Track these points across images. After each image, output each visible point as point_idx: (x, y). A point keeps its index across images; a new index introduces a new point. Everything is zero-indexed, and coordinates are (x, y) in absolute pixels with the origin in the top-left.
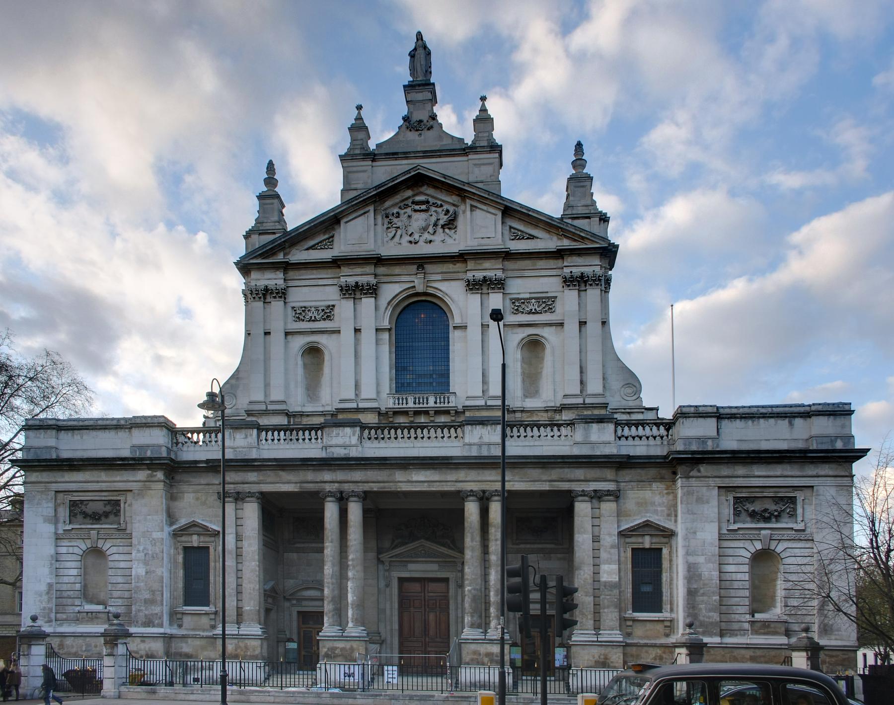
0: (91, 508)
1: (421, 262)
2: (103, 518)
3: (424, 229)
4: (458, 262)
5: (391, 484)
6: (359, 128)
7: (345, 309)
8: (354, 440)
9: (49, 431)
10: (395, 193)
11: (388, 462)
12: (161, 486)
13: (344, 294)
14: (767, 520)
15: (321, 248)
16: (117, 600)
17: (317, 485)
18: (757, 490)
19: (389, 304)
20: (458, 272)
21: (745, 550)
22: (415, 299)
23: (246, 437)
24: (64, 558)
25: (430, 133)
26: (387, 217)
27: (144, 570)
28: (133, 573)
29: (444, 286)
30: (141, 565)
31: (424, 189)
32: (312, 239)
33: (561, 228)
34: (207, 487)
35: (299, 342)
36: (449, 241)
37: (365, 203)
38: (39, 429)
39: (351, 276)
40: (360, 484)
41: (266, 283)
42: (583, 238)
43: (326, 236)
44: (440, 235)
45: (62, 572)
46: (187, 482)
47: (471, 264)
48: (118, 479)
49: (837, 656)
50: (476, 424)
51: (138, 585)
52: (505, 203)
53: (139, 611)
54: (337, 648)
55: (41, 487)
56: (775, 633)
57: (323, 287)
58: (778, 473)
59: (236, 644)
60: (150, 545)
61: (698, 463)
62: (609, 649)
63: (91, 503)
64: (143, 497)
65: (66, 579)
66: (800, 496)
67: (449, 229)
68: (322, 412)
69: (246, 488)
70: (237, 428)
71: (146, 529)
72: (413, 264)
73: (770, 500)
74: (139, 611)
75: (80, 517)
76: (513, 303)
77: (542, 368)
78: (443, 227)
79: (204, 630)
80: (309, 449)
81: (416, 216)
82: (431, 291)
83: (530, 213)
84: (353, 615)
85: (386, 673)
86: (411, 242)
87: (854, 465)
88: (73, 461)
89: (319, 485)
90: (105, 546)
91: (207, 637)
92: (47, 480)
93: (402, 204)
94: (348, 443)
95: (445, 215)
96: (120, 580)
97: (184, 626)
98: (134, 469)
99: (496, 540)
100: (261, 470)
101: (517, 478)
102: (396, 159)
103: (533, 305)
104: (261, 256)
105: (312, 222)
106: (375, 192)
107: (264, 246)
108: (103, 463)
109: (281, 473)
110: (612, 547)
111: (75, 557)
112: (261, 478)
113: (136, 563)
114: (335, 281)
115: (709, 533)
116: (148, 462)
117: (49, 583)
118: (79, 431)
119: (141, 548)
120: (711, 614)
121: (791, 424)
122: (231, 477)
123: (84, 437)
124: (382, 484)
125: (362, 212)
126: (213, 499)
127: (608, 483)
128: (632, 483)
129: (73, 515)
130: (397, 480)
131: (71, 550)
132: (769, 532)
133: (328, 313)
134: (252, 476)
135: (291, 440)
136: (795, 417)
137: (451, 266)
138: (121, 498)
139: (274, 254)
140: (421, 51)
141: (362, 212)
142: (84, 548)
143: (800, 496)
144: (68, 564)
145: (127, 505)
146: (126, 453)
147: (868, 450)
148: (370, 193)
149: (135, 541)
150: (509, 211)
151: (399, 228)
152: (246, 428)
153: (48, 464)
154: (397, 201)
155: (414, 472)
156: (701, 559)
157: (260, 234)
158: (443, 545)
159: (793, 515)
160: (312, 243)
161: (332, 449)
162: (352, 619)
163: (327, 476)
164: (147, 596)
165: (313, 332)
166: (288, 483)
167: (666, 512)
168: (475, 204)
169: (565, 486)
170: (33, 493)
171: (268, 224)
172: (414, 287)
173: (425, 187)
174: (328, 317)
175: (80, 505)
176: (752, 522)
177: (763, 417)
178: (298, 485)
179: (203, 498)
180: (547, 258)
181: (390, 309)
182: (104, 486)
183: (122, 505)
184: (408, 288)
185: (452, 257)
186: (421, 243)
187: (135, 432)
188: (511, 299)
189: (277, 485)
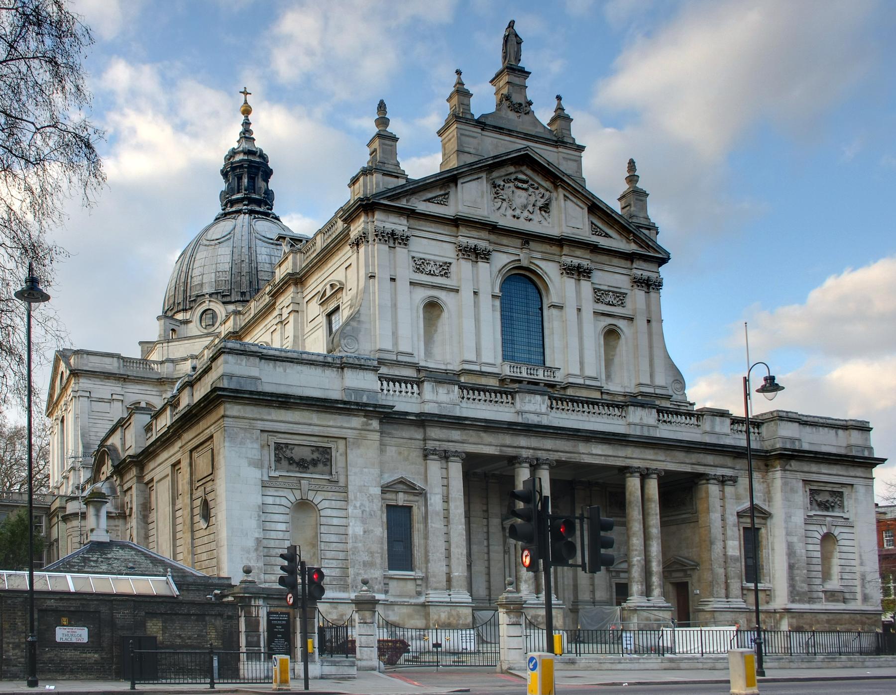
0: (298, 453)
1: (527, 238)
2: (310, 466)
3: (525, 207)
4: (554, 244)
5: (576, 455)
6: (461, 93)
7: (463, 269)
8: (544, 408)
9: (252, 358)
11: (579, 434)
12: (376, 436)
14: (827, 509)
15: (438, 203)
16: (331, 561)
17: (514, 449)
18: (822, 484)
19: (500, 271)
20: (555, 255)
21: (818, 532)
22: (516, 272)
23: (448, 393)
24: (270, 509)
25: (526, 117)
26: (495, 187)
27: (362, 528)
28: (350, 531)
29: (542, 264)
30: (359, 523)
31: (524, 168)
33: (634, 234)
34: (410, 441)
35: (422, 294)
36: (544, 223)
37: (481, 169)
38: (241, 354)
40: (551, 453)
41: (394, 227)
42: (649, 246)
43: (442, 192)
44: (537, 216)
45: (269, 526)
46: (389, 434)
47: (566, 250)
48: (331, 423)
49: (871, 618)
50: (637, 406)
51: (356, 545)
52: (594, 201)
53: (358, 574)
54: (539, 616)
55: (243, 424)
56: (837, 601)
57: (440, 243)
58: (834, 472)
59: (448, 612)
60: (367, 502)
61: (791, 459)
62: (738, 614)
63: (296, 447)
64: (359, 447)
65: (273, 535)
66: (846, 491)
68: (446, 370)
69: (451, 447)
70: (440, 382)
71: (362, 483)
72: (519, 238)
73: (827, 493)
74: (358, 574)
75: (284, 463)
76: (595, 292)
77: (613, 355)
78: (540, 209)
79: (411, 597)
80: (502, 412)
81: (519, 192)
82: (533, 267)
83: (613, 215)
85: (624, 639)
86: (514, 216)
87: (874, 470)
88: (290, 398)
89: (517, 450)
90: (317, 498)
91: (415, 605)
92: (250, 416)
93: (506, 178)
94: (538, 411)
96: (333, 538)
97: (390, 591)
98: (349, 415)
99: (656, 514)
100: (465, 429)
101: (668, 459)
102: (501, 134)
104: (388, 198)
106: (492, 162)
107: (395, 189)
108: (323, 404)
109: (483, 434)
110: (734, 525)
111: (282, 510)
112: (465, 438)
113: (353, 521)
114: (453, 240)
115: (799, 517)
116: (371, 409)
117: (257, 538)
118: (281, 363)
119: (358, 505)
120: (803, 585)
121: (837, 434)
122: (435, 432)
123: (288, 371)
124: (569, 455)
125: (476, 176)
126: (416, 455)
127: (728, 469)
128: (741, 471)
129: (278, 460)
130: (581, 451)
131: (278, 500)
132: (831, 519)
133: (445, 269)
134: (456, 435)
135: (480, 400)
136: (839, 428)
137: (548, 247)
138: (333, 446)
139: (399, 198)
140: (512, 38)
142: (293, 499)
143: (846, 491)
144: (276, 518)
145: (338, 454)
146: (336, 395)
147: (886, 459)
149: (351, 496)
150: (595, 208)
152: (449, 383)
153: (261, 397)
154: (503, 174)
156: (795, 539)
157: (384, 174)
159: (842, 506)
160: (430, 195)
161: (527, 415)
163: (523, 441)
164: (366, 558)
165: (434, 287)
166: (490, 445)
167: (763, 498)
168: (567, 195)
169: (701, 469)
170: (235, 429)
171: (390, 166)
172: (519, 260)
174: (446, 273)
175: (284, 450)
176: (819, 510)
177: (822, 426)
178: (498, 448)
179: (406, 453)
180: (620, 257)
182: (316, 430)
183: (333, 454)
184: (515, 261)
185: (552, 239)
186: (522, 219)
187: (348, 373)
188: (594, 289)
189: (480, 446)
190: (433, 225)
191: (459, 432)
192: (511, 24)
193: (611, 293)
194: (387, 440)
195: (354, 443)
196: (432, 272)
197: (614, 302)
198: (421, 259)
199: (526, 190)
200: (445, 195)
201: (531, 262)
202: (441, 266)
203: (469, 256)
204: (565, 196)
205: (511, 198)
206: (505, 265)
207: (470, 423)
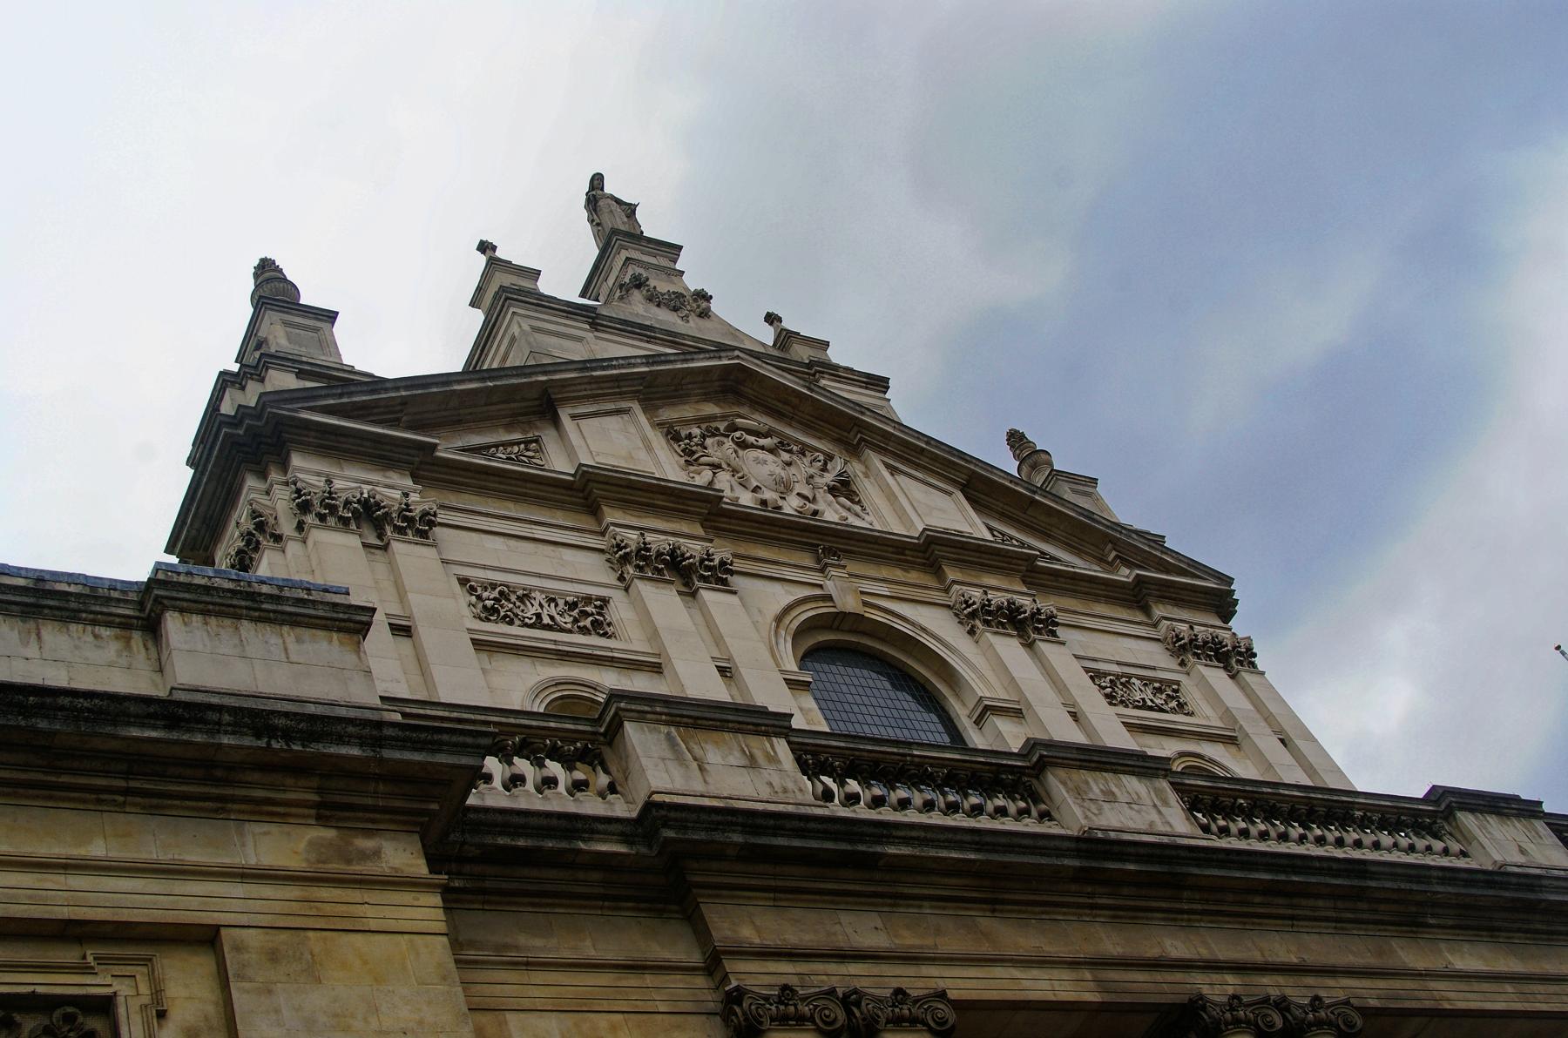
10: (681, 396)
34: (632, 980)
125: (611, 406)
141: (611, 406)
148: (635, 365)
151: (719, 466)
191: (874, 920)
192: (597, 181)
193: (1133, 680)
194: (504, 984)
195: (273, 956)
196: (546, 620)
197: (1158, 701)
198: (494, 586)
199: (771, 451)
200: (527, 443)
201: (865, 604)
202: (573, 606)
203: (660, 571)
204: (887, 466)
205: (733, 463)
206: (788, 609)
207: (905, 851)
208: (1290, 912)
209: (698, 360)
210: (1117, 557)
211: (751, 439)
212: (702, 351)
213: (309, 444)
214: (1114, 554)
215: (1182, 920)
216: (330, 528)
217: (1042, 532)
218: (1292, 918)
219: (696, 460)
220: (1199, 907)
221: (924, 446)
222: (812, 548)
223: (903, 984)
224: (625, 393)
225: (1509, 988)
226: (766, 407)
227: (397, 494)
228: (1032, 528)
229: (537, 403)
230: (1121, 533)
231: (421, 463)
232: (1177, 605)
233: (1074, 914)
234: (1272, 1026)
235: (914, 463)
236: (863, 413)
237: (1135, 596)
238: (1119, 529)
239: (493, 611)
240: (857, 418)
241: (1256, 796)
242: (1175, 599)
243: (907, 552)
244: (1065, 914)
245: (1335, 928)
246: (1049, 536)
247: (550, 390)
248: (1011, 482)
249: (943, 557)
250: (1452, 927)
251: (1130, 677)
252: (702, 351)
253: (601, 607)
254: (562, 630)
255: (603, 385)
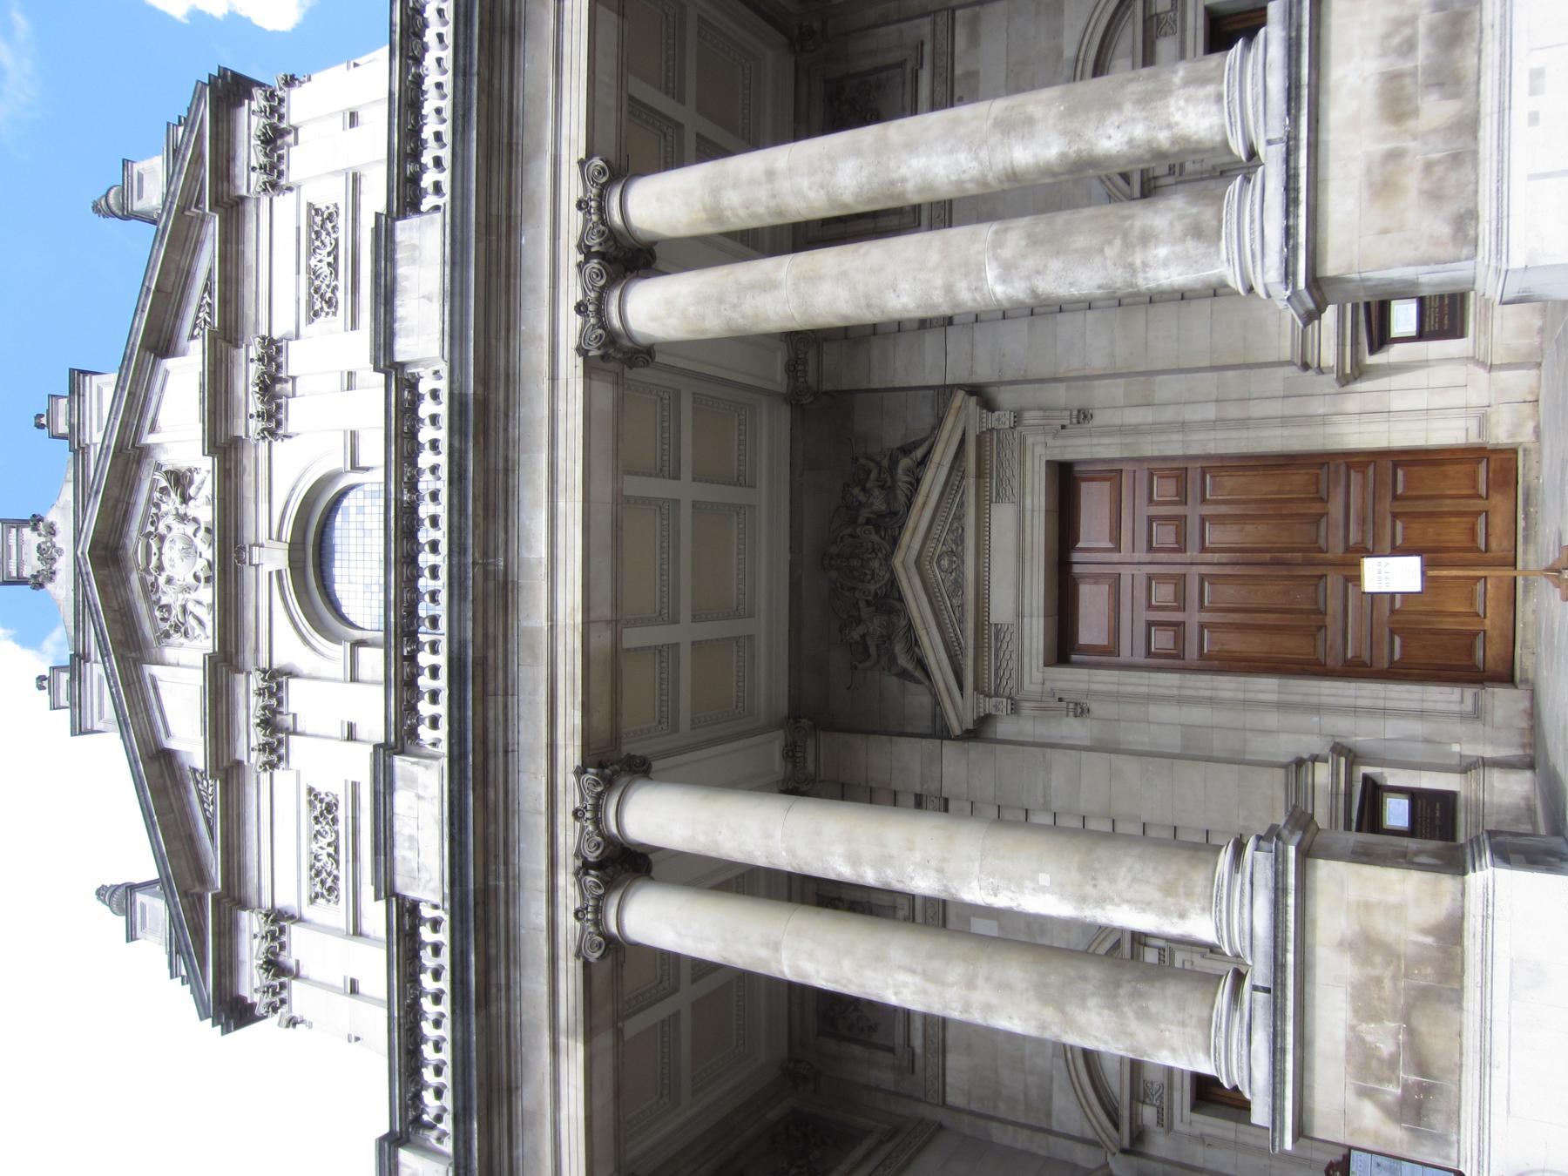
13: (280, 758)
26: (167, 635)
32: (196, 825)
39: (248, 740)
67: (191, 482)
76: (316, 314)
78: (185, 499)
84: (1145, 905)
95: (169, 495)
103: (320, 261)
105: (151, 817)
141: (151, 692)
148: (112, 670)
155: (524, 553)
158: (916, 483)
162: (1166, 912)
173: (127, 541)
181: (317, 639)
188: (310, 321)
190: (248, 828)
200: (198, 782)
208: (501, 754)
209: (94, 599)
210: (196, 207)
211: (154, 559)
212: (85, 595)
213: (231, 982)
214: (193, 209)
215: (514, 886)
216: (290, 995)
217: (187, 278)
218: (506, 752)
219: (183, 624)
220: (502, 868)
221: (126, 393)
222: (238, 572)
223: (572, 304)
224: (138, 677)
225: (561, 504)
226: (124, 521)
227: (256, 942)
228: (184, 289)
229: (162, 761)
230: (172, 203)
231: (225, 339)
232: (234, 159)
233: (515, 1004)
234: (601, 336)
235: (145, 401)
236: (108, 447)
237: (232, 207)
238: (168, 204)
239: (330, 890)
240: (114, 453)
241: (398, 632)
242: (228, 161)
243: (227, 467)
244: (515, 1015)
245: (513, 695)
246: (189, 272)
247: (150, 754)
248: (143, 311)
249: (226, 434)
250: (506, 532)
251: (308, 266)
252: (85, 595)
253: (315, 796)
254: (336, 246)
255: (136, 700)
